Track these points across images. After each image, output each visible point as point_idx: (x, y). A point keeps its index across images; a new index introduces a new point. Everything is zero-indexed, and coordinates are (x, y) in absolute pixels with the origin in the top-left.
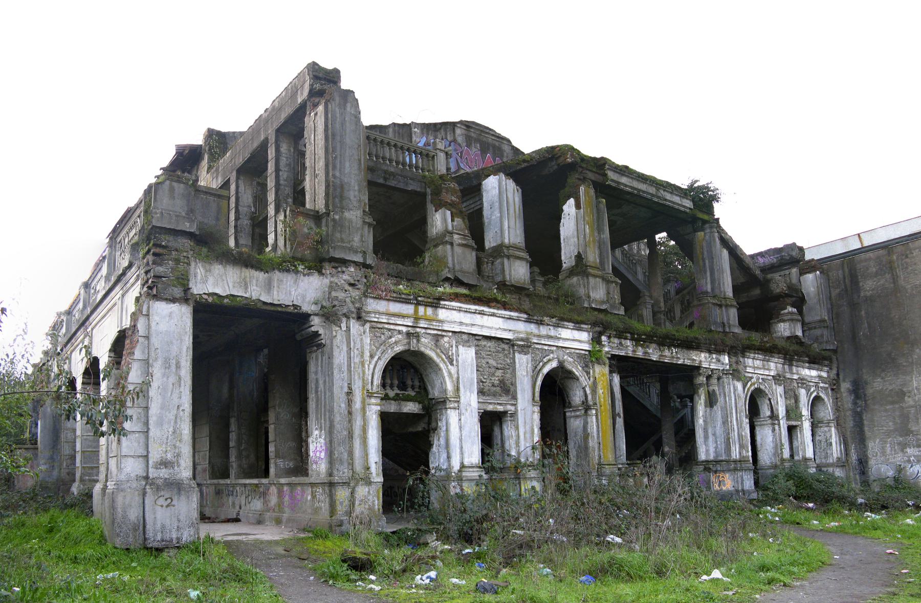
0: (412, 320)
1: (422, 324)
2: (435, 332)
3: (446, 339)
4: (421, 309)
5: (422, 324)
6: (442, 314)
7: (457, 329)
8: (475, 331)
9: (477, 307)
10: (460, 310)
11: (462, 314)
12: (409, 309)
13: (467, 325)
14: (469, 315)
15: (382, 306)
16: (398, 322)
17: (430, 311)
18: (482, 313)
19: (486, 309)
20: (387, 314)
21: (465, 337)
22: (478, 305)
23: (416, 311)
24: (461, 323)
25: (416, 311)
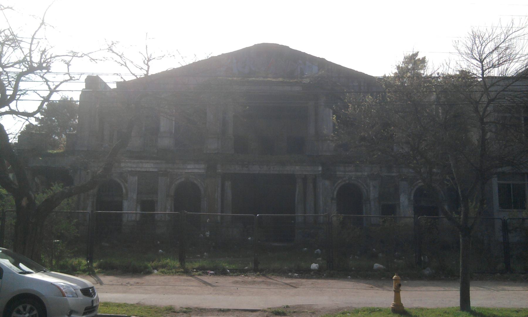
7: (130, 169)
8: (138, 169)
18: (141, 162)
24: (132, 167)
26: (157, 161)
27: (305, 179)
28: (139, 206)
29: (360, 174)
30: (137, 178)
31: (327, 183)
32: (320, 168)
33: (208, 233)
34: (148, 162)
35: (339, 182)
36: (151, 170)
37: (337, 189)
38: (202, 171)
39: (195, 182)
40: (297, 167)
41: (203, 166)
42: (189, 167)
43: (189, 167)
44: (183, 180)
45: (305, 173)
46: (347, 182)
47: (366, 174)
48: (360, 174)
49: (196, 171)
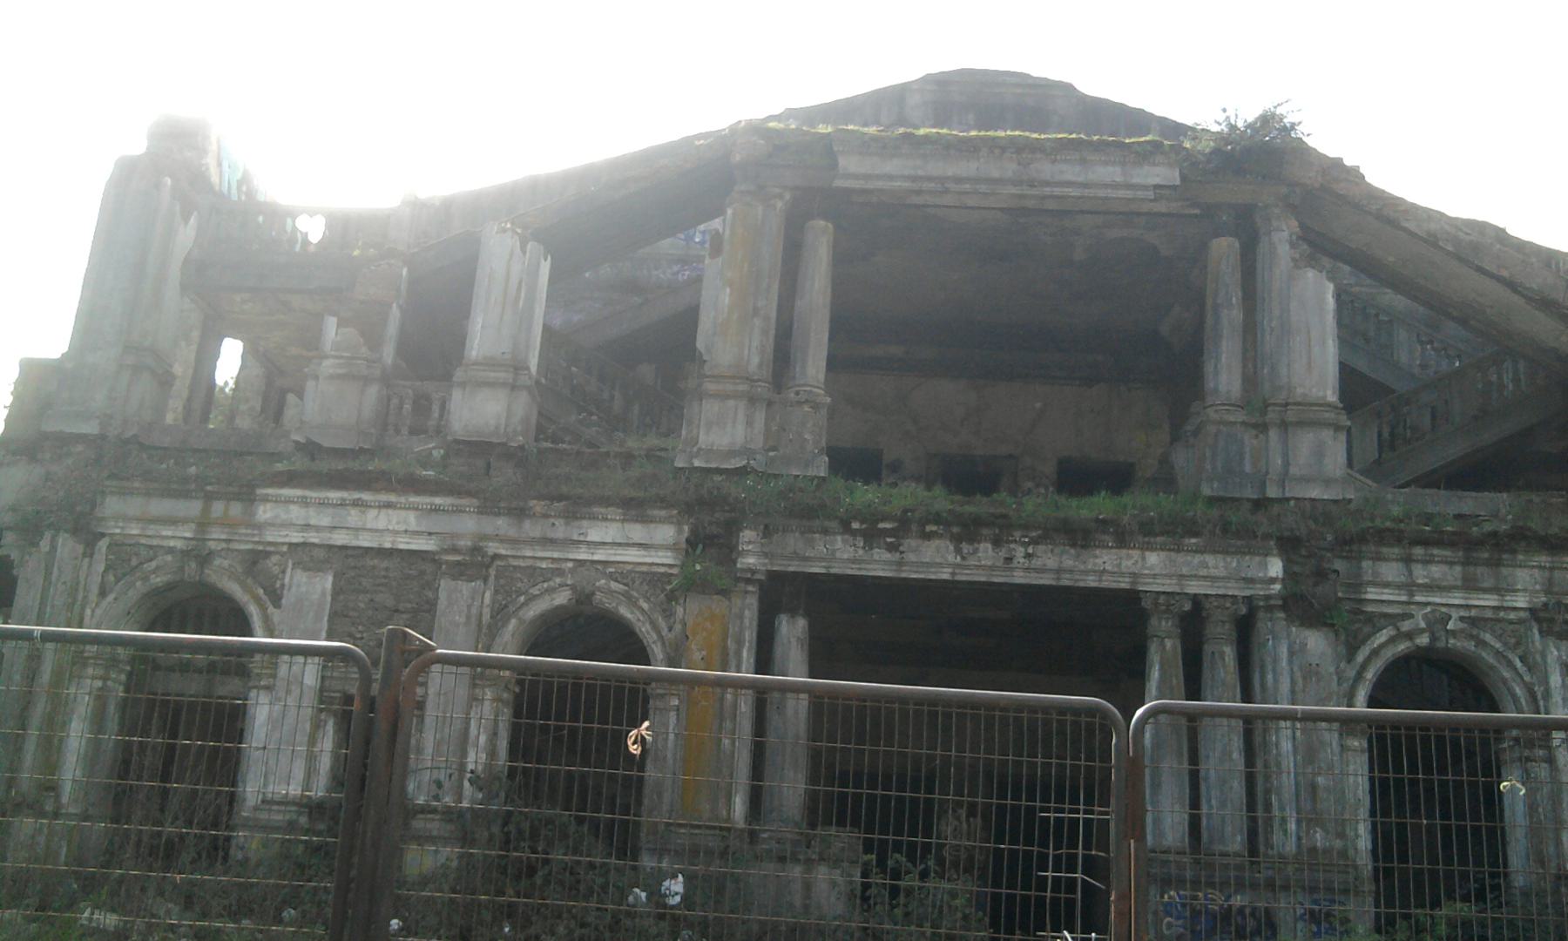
0: (193, 526)
1: (217, 533)
2: (249, 546)
3: (275, 559)
4: (218, 508)
5: (217, 533)
6: (264, 513)
7: (296, 538)
8: (340, 538)
9: (345, 494)
10: (304, 502)
11: (312, 512)
12: (193, 508)
13: (318, 529)
14: (330, 510)
15: (134, 506)
16: (164, 533)
17: (236, 509)
18: (356, 504)
19: (366, 496)
20: (138, 520)
21: (316, 553)
22: (345, 488)
23: (206, 510)
24: (307, 527)
25: (206, 510)
26: (438, 500)
27: (1193, 620)
28: (330, 727)
29: (1490, 600)
30: (328, 581)
31: (1316, 642)
32: (1275, 567)
33: (676, 886)
34: (389, 505)
35: (1382, 637)
36: (403, 544)
37: (1370, 675)
38: (665, 558)
39: (625, 612)
40: (1153, 558)
41: (666, 533)
42: (595, 535)
43: (595, 535)
44: (562, 598)
45: (1194, 588)
46: (1423, 640)
47: (1521, 602)
48: (1490, 600)
49: (632, 556)
